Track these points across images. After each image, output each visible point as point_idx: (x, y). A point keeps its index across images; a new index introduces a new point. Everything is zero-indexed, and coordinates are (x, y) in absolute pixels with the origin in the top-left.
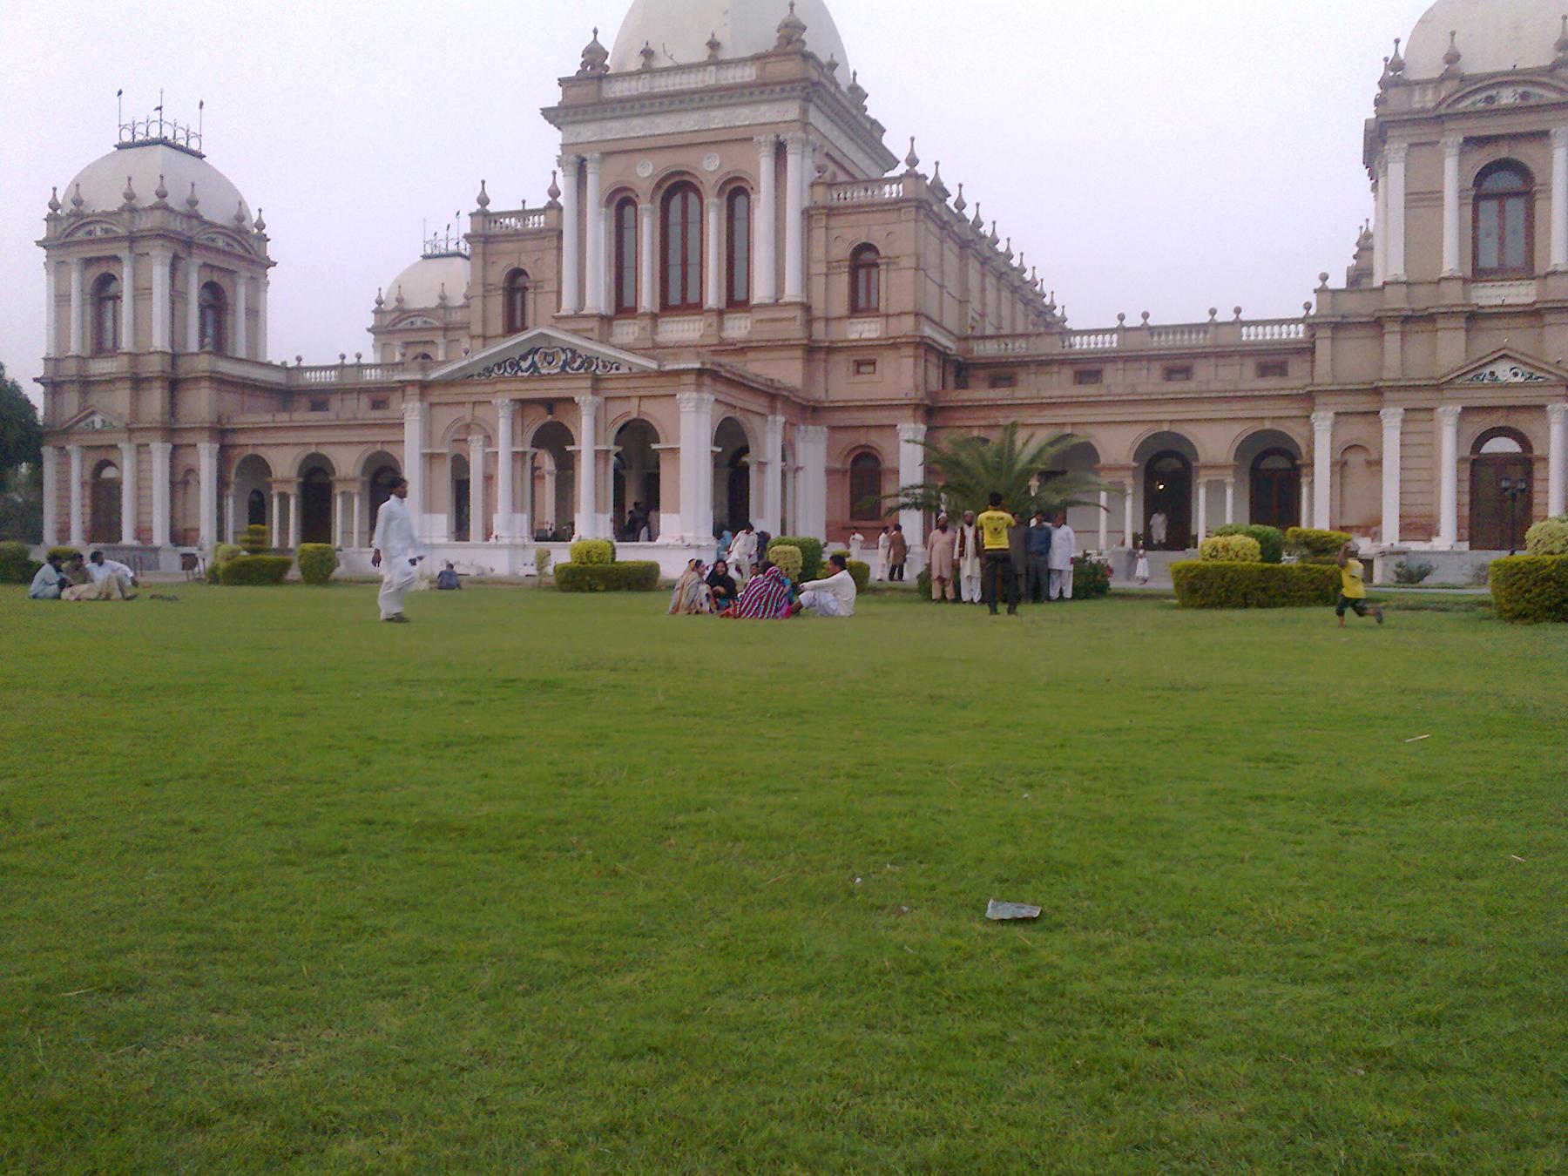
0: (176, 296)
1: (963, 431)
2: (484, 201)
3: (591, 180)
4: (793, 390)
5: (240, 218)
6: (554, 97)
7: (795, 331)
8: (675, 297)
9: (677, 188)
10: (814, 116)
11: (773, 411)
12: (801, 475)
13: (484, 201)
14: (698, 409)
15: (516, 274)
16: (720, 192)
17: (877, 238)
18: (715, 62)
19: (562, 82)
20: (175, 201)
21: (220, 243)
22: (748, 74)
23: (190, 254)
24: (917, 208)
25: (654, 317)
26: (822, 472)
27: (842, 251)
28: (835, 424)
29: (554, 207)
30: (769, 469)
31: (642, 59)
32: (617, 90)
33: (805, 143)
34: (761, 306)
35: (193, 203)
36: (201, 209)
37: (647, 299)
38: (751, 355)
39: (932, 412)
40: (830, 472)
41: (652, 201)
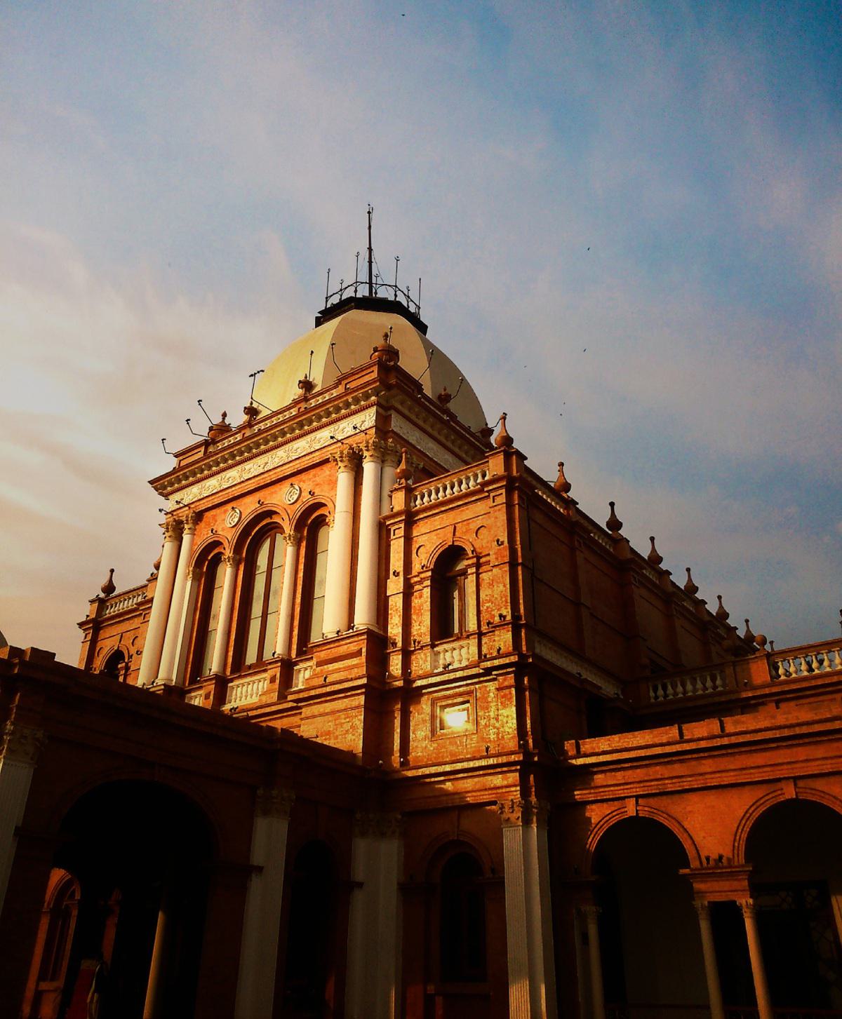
1: (606, 809)
2: (109, 588)
3: (186, 538)
4: (351, 754)
7: (355, 670)
8: (251, 657)
9: (259, 530)
10: (397, 424)
13: (109, 588)
15: (117, 656)
16: (299, 525)
17: (467, 541)
24: (509, 491)
26: (395, 887)
29: (154, 578)
30: (256, 885)
34: (327, 643)
40: (405, 889)
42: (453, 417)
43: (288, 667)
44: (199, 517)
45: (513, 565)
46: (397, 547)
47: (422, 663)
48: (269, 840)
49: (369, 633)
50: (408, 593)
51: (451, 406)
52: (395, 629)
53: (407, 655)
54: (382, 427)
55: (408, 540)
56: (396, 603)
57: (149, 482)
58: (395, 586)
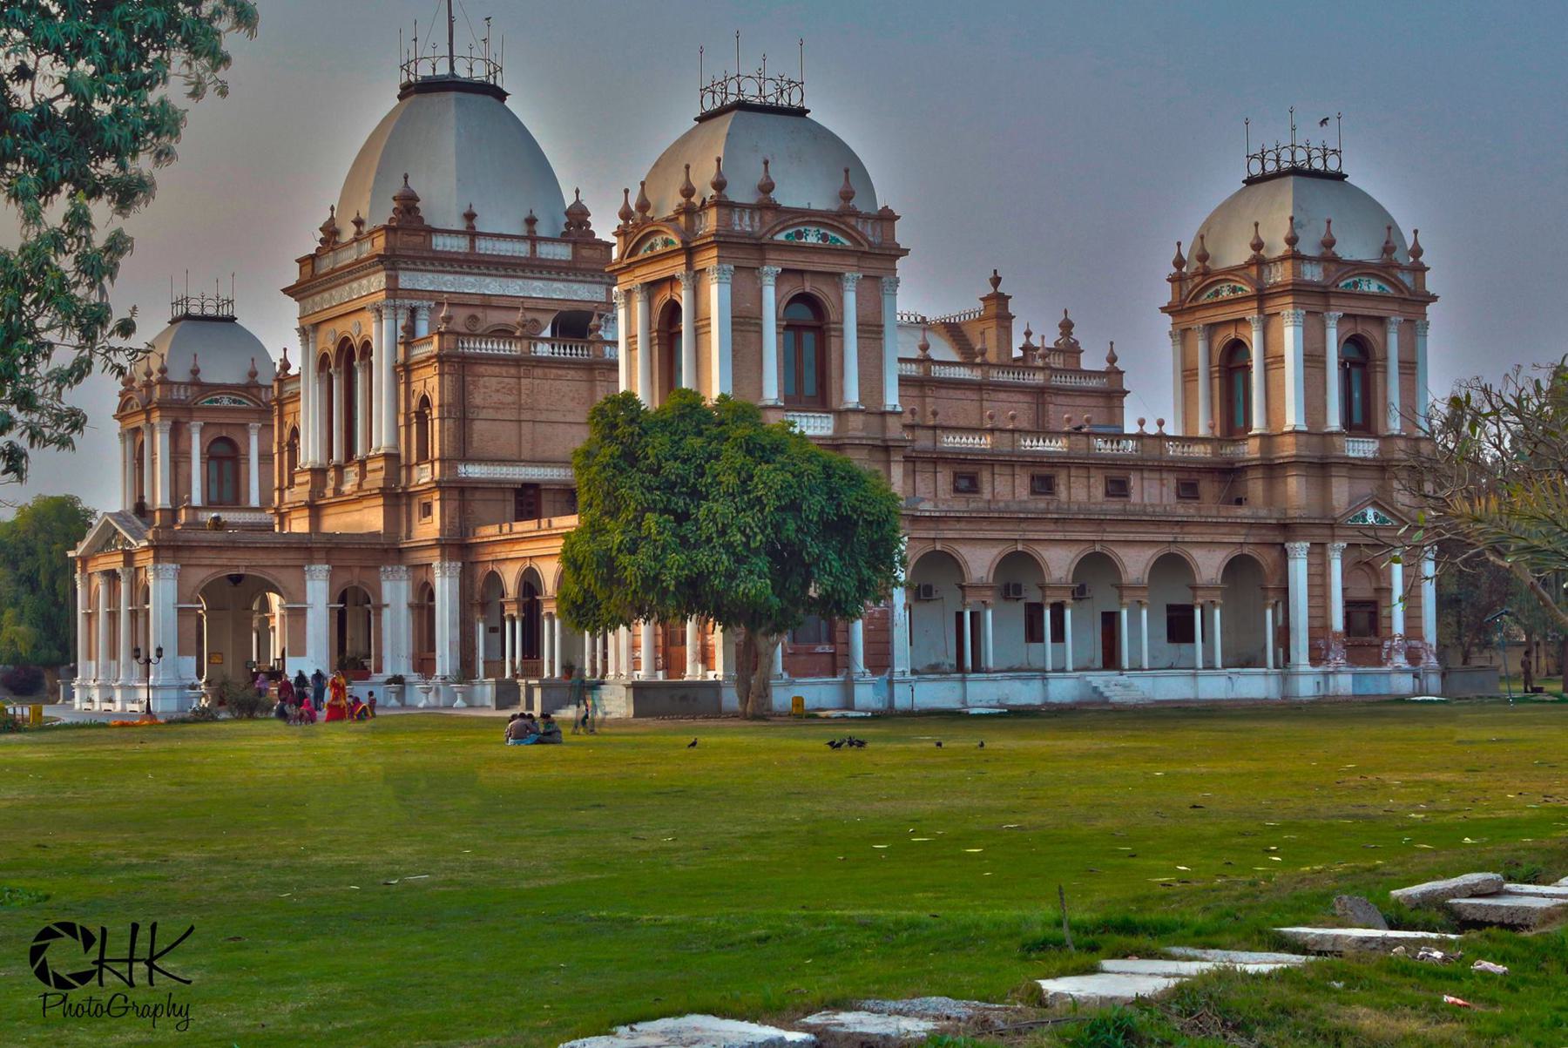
0: (178, 458)
4: (375, 535)
5: (253, 374)
6: (293, 276)
11: (311, 562)
12: (386, 613)
14: (157, 575)
18: (358, 238)
19: (301, 261)
20: (179, 374)
21: (226, 402)
22: (367, 249)
23: (191, 419)
25: (339, 469)
27: (415, 403)
28: (416, 562)
30: (310, 614)
31: (354, 228)
32: (326, 265)
33: (395, 308)
35: (195, 372)
36: (207, 377)
37: (337, 456)
38: (365, 503)
39: (459, 546)
40: (410, 606)
41: (337, 366)
42: (472, 234)
43: (363, 463)
44: (316, 326)
45: (442, 419)
46: (402, 387)
47: (415, 471)
48: (318, 590)
49: (385, 455)
50: (408, 426)
51: (475, 222)
52: (403, 454)
53: (409, 467)
54: (393, 290)
55: (408, 383)
56: (403, 430)
57: (285, 291)
58: (402, 421)
